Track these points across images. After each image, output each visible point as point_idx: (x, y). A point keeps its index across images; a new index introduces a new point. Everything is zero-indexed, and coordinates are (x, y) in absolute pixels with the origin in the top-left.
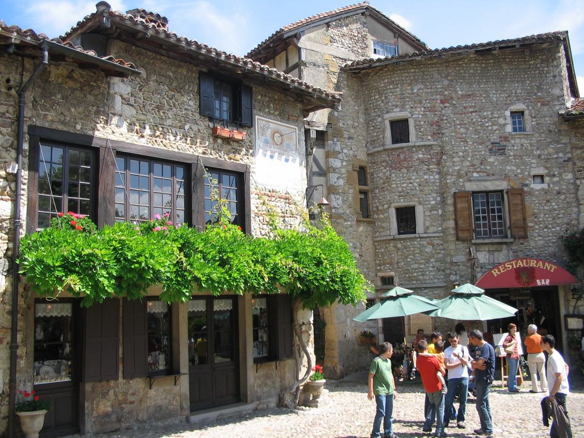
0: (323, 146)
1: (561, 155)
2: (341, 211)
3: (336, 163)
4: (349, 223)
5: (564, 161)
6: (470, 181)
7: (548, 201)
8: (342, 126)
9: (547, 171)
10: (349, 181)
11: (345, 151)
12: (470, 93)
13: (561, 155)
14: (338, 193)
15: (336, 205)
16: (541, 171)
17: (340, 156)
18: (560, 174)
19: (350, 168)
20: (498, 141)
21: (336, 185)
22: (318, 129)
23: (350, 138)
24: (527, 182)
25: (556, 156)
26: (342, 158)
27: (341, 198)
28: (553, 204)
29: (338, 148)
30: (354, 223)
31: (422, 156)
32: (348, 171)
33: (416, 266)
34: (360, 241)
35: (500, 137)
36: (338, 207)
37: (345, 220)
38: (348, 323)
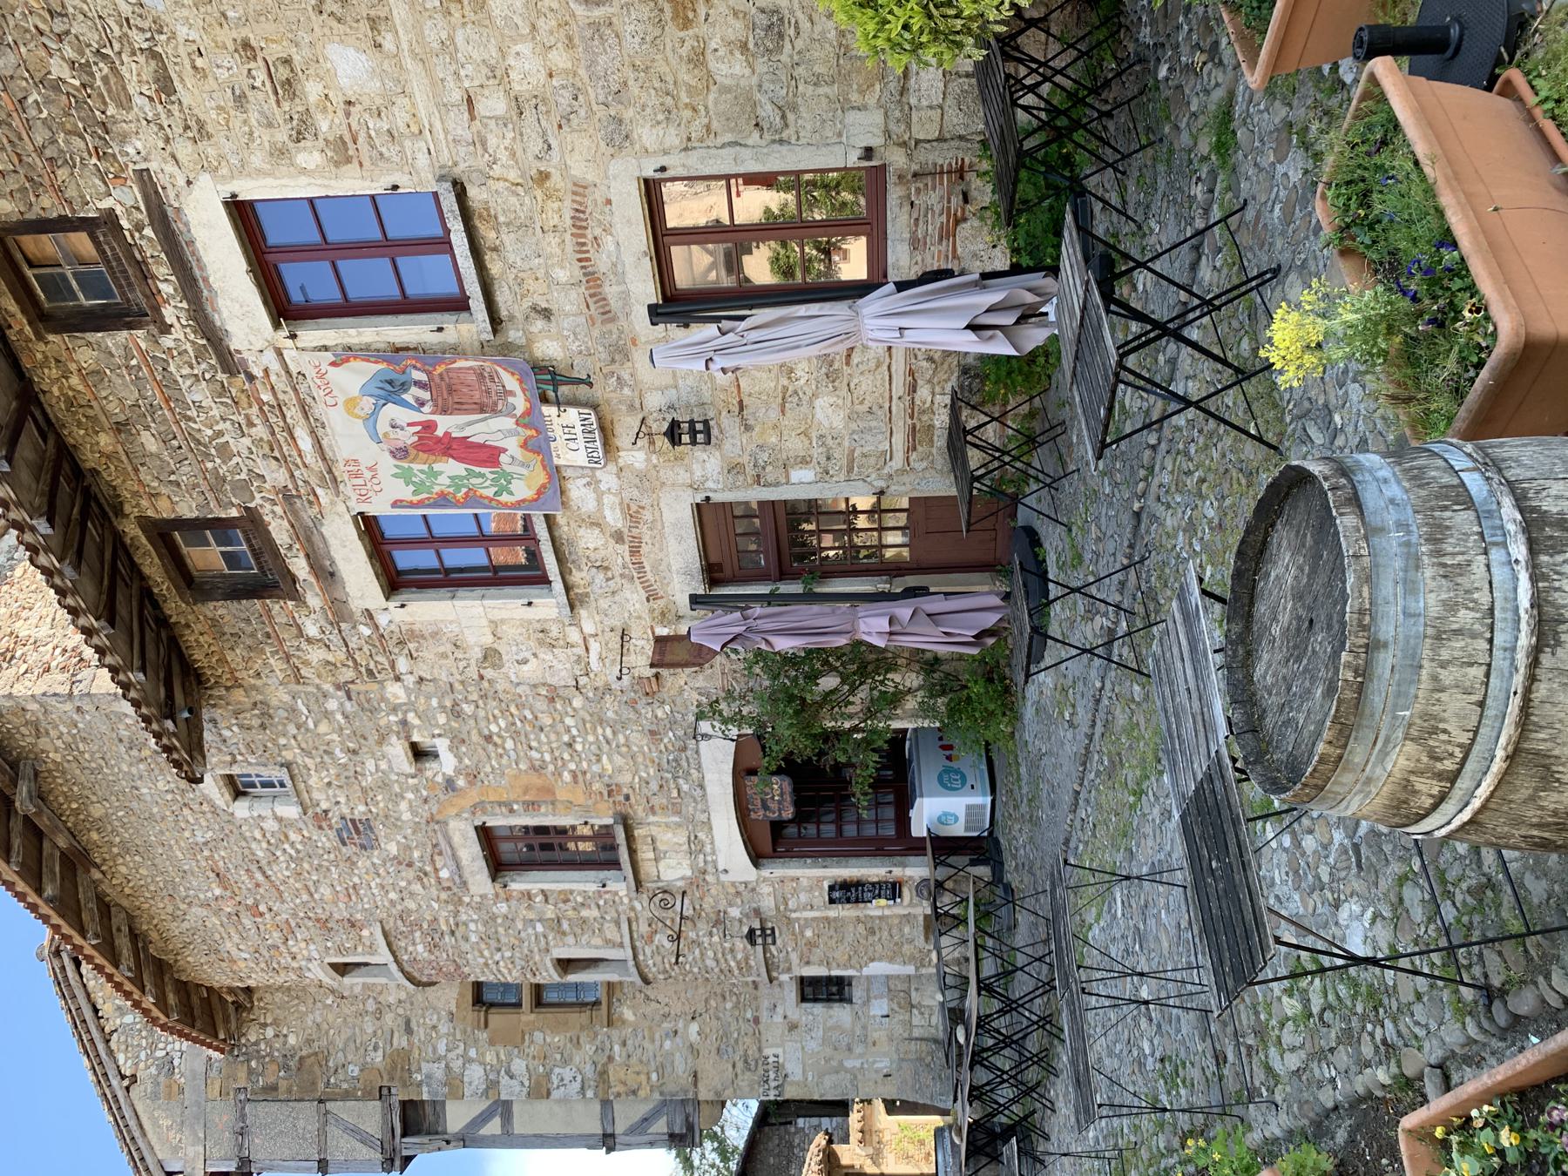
0: (438, 1106)
1: (332, 705)
2: (589, 1070)
3: (475, 1075)
4: (617, 1048)
5: (350, 698)
6: (465, 883)
7: (488, 738)
8: (380, 1053)
9: (394, 739)
10: (516, 1040)
11: (442, 1049)
12: (212, 875)
13: (332, 705)
14: (548, 1075)
15: (577, 1086)
16: (398, 751)
17: (457, 1065)
18: (394, 709)
19: (483, 1036)
20: (332, 834)
21: (527, 1083)
22: (398, 1131)
23: (409, 1030)
24: (439, 779)
25: (339, 717)
26: (460, 1062)
27: (557, 1070)
28: (494, 728)
29: (438, 1071)
30: (615, 1033)
31: (420, 948)
32: (492, 1042)
33: (710, 963)
34: (657, 1018)
35: (320, 828)
36: (579, 1078)
37: (611, 1059)
38: (857, 1063)
